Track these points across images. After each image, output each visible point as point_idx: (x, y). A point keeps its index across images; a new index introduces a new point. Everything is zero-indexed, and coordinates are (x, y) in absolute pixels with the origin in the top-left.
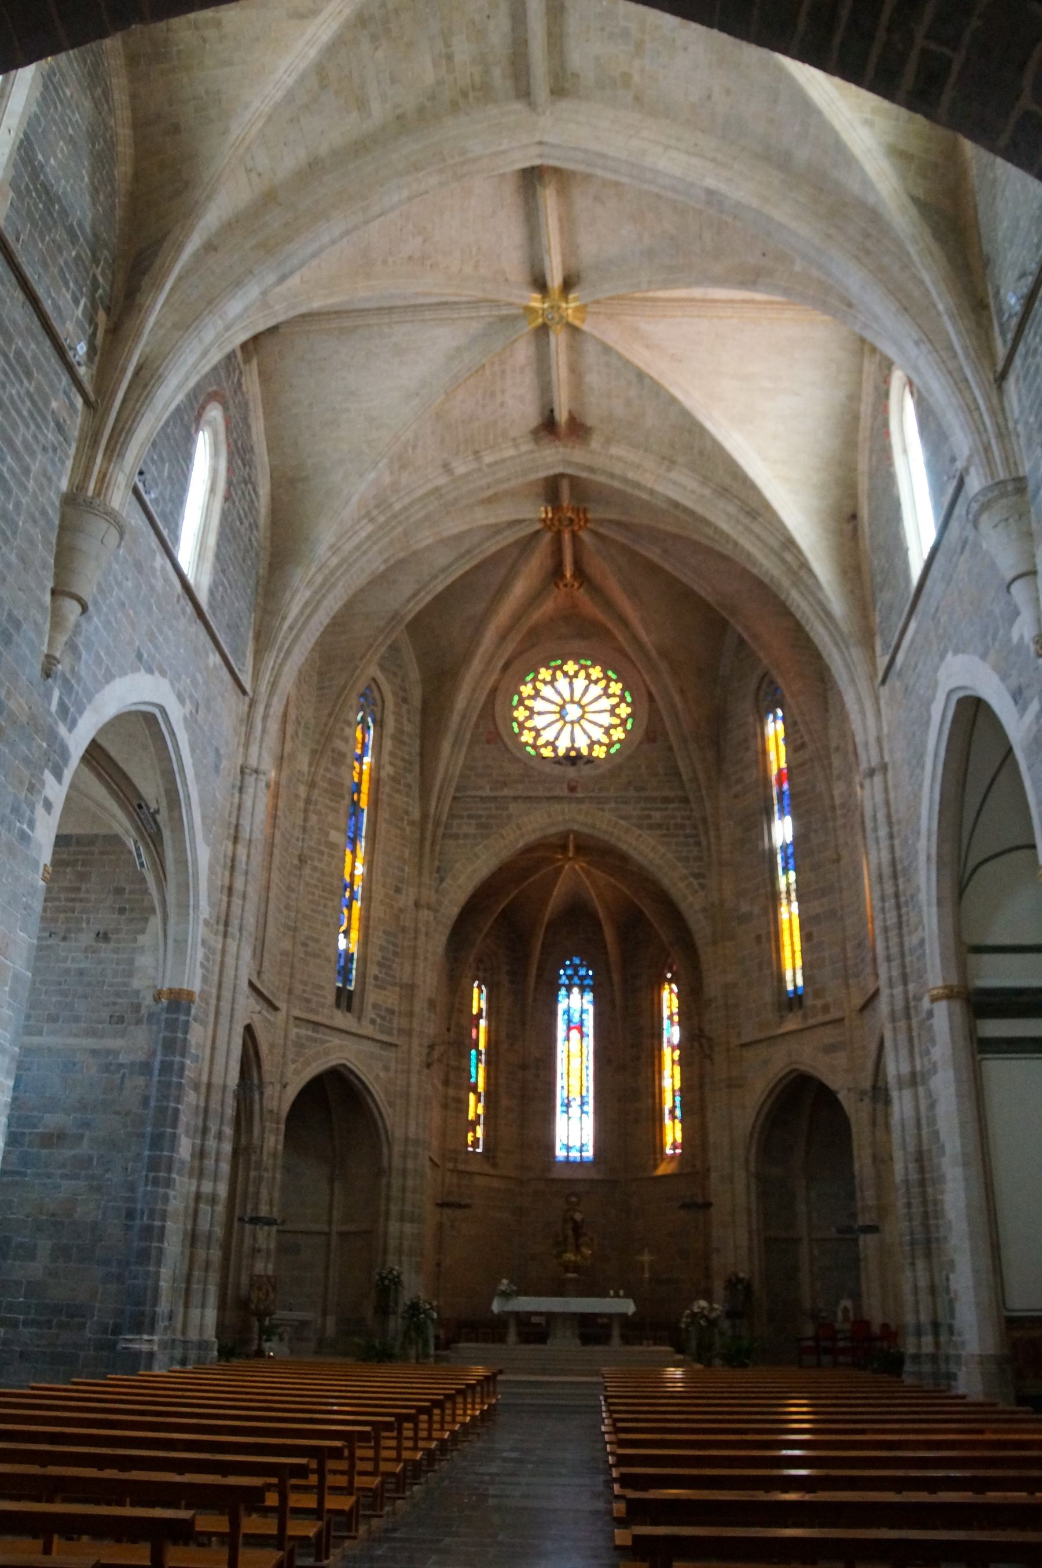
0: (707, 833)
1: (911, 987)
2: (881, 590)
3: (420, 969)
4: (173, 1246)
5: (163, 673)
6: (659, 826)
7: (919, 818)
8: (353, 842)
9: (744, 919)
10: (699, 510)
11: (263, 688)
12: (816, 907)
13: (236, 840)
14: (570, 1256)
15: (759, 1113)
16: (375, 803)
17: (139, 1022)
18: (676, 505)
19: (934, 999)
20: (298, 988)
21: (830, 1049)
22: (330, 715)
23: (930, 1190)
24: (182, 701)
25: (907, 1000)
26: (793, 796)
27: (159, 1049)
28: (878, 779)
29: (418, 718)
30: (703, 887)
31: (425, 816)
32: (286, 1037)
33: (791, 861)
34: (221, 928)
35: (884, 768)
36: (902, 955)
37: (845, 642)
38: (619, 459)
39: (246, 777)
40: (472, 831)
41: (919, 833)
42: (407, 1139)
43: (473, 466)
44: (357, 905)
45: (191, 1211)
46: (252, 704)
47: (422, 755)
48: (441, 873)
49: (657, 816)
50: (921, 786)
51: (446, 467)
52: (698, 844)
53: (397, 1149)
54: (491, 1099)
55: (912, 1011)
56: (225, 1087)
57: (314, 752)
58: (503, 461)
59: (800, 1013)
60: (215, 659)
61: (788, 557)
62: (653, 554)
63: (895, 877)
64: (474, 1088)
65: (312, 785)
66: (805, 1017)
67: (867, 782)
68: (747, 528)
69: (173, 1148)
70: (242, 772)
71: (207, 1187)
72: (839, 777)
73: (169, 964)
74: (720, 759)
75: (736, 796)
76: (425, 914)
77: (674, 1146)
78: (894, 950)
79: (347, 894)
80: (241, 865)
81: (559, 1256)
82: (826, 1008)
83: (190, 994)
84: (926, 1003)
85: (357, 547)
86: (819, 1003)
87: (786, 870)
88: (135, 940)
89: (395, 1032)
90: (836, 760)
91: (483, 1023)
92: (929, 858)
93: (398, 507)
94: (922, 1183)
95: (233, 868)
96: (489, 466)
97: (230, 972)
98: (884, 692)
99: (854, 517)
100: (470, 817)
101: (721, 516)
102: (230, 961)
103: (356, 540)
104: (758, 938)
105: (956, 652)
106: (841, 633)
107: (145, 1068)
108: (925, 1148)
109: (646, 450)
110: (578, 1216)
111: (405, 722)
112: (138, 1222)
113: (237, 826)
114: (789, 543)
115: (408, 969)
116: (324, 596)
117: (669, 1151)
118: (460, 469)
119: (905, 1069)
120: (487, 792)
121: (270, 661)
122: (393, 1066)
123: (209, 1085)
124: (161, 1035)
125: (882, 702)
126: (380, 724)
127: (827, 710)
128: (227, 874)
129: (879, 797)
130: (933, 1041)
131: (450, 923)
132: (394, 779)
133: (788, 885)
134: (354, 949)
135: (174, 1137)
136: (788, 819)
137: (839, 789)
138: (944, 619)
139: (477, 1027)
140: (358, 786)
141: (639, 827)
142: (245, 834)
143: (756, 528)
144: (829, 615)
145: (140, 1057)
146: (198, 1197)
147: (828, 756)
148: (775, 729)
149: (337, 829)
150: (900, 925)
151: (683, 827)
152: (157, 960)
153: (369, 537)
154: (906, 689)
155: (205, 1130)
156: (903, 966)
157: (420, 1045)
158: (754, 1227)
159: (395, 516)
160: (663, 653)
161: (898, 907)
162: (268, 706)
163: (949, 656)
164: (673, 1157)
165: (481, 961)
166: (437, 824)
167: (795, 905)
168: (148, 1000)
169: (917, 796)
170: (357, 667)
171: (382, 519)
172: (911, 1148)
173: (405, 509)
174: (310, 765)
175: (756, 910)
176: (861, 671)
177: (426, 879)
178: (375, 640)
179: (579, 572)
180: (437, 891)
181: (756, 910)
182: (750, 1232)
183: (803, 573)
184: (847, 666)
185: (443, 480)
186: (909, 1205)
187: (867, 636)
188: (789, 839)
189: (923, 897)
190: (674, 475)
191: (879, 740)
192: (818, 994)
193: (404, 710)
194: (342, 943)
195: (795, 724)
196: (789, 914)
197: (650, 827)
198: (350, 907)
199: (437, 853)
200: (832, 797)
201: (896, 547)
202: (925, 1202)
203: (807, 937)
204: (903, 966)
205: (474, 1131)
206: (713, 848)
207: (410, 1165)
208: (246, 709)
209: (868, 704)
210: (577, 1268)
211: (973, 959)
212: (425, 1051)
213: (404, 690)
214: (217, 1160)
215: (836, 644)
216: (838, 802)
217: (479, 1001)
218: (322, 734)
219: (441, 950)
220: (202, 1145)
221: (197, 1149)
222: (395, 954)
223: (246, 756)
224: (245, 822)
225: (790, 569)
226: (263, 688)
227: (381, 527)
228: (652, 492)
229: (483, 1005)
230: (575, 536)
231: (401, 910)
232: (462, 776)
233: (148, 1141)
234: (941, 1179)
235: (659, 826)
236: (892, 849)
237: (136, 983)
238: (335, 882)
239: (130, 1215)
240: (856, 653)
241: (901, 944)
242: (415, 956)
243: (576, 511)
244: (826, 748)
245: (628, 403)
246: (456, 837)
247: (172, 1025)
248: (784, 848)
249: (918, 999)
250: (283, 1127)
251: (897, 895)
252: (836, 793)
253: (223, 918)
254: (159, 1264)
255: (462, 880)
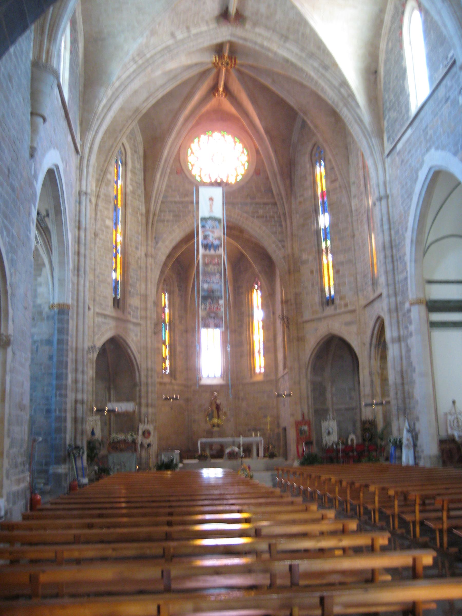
0: (285, 220)
1: (399, 298)
2: (389, 110)
3: (149, 286)
4: (69, 425)
5: (58, 149)
6: (262, 217)
7: (407, 223)
8: (116, 224)
9: (306, 262)
10: (299, 64)
11: (87, 151)
12: (341, 258)
13: (79, 228)
14: (215, 421)
15: (312, 353)
16: (125, 205)
17: (43, 319)
18: (287, 61)
19: (412, 304)
20: (97, 298)
21: (348, 324)
22: (105, 161)
23: (406, 387)
24: (63, 162)
25: (396, 304)
26: (329, 205)
27: (56, 332)
28: (384, 202)
29: (142, 161)
30: (283, 246)
31: (148, 212)
32: (94, 323)
33: (329, 236)
34: (76, 272)
35: (387, 197)
36: (395, 284)
37: (369, 135)
38: (260, 35)
39: (82, 197)
40: (171, 218)
41: (406, 229)
42: (147, 369)
43: (186, 35)
44: (119, 256)
45: (73, 408)
46: (81, 159)
47: (145, 180)
48: (157, 240)
49: (261, 212)
50: (409, 208)
51: (173, 35)
52: (281, 226)
53: (143, 374)
54: (172, 348)
55: (399, 309)
56: (83, 350)
57: (98, 180)
58: (201, 33)
59: (333, 307)
60: (70, 138)
61: (343, 90)
62: (267, 82)
63: (392, 247)
64: (164, 343)
65: (98, 197)
66: (335, 309)
67: (378, 204)
68: (322, 75)
69: (67, 379)
70: (79, 193)
71: (79, 397)
72: (355, 196)
73: (57, 290)
74: (292, 185)
75: (300, 203)
76: (150, 260)
77: (260, 367)
78: (391, 281)
79: (114, 251)
80: (83, 241)
81: (210, 420)
82: (346, 305)
83: (68, 306)
84: (407, 305)
85: (129, 77)
86: (343, 303)
87: (325, 239)
88: (36, 280)
89: (139, 317)
90: (353, 189)
91: (167, 310)
92: (412, 241)
93: (148, 56)
94: (403, 384)
95: (79, 243)
96: (196, 35)
97: (82, 294)
98: (388, 161)
99: (376, 72)
100: (169, 211)
101: (310, 69)
102: (81, 288)
103: (128, 73)
104: (312, 272)
105: (437, 148)
106: (367, 131)
107: (49, 342)
108: (404, 369)
109: (273, 31)
110: (218, 402)
111: (136, 162)
112: (53, 415)
113: (79, 222)
114: (344, 83)
115: (143, 286)
116: (113, 103)
117: (258, 371)
118: (180, 36)
119: (395, 334)
120: (177, 199)
121: (90, 137)
122: (139, 334)
123: (77, 349)
124: (56, 326)
125: (387, 166)
126: (125, 164)
127: (349, 163)
128: (77, 246)
129: (384, 211)
130: (411, 323)
131: (162, 264)
132: (133, 192)
133: (327, 248)
134: (119, 279)
135: (67, 374)
136: (327, 215)
137: (354, 202)
138: (430, 132)
139: (164, 313)
140: (116, 197)
141: (253, 217)
142: (83, 225)
143: (327, 75)
144: (361, 121)
145: (45, 337)
146: (76, 402)
147: (349, 186)
148: (320, 171)
149: (109, 218)
150: (393, 270)
151: (273, 217)
152: (49, 290)
153: (134, 71)
154: (403, 161)
155: (76, 370)
156: (395, 288)
157: (151, 324)
158: (310, 403)
159: (147, 60)
160: (267, 132)
161: (393, 262)
162: (88, 160)
163: (433, 150)
164: (260, 373)
165: (165, 280)
166: (154, 215)
167: (330, 256)
168: (46, 309)
169: (407, 212)
170: (117, 137)
171: (140, 62)
172: (398, 368)
173: (152, 57)
174: (96, 186)
175: (311, 258)
176: (377, 149)
177: (149, 242)
178: (127, 121)
179: (226, 88)
180: (155, 248)
181: (311, 258)
182: (308, 406)
183: (350, 100)
184: (369, 146)
185: (171, 42)
186: (396, 394)
187: (380, 133)
188: (327, 225)
189: (407, 258)
190: (287, 45)
191: (385, 183)
192: (342, 298)
193: (136, 158)
194: (114, 275)
195: (333, 168)
196: (327, 261)
197: (258, 217)
198: (116, 257)
199: (154, 230)
200: (351, 206)
201: (401, 92)
202: (404, 392)
203: (336, 272)
204: (395, 288)
205: (165, 362)
206: (289, 229)
207: (150, 381)
208: (79, 161)
209: (380, 166)
210: (218, 426)
211: (428, 287)
212: (153, 326)
213: (135, 146)
214: (83, 384)
215: (365, 135)
216: (353, 208)
217: (165, 300)
218: (102, 171)
219: (157, 277)
220: (76, 378)
221: (74, 379)
222: (137, 279)
223: (80, 185)
224: (83, 220)
225: (343, 97)
226: (87, 151)
227: (140, 66)
228: (275, 54)
229: (167, 303)
230: (227, 71)
231: (138, 258)
232: (166, 191)
233: (55, 376)
234: (412, 383)
235: (262, 217)
236: (390, 235)
237: (39, 301)
238: (110, 245)
239: (48, 411)
240: (375, 141)
241: (394, 279)
242: (146, 281)
243: (230, 58)
244: (349, 183)
245: (269, 6)
246: (163, 221)
247: (61, 321)
248: (325, 229)
249: (403, 303)
250: (95, 365)
251: (392, 256)
252: (353, 204)
253: (76, 267)
254: (65, 433)
255: (167, 243)
